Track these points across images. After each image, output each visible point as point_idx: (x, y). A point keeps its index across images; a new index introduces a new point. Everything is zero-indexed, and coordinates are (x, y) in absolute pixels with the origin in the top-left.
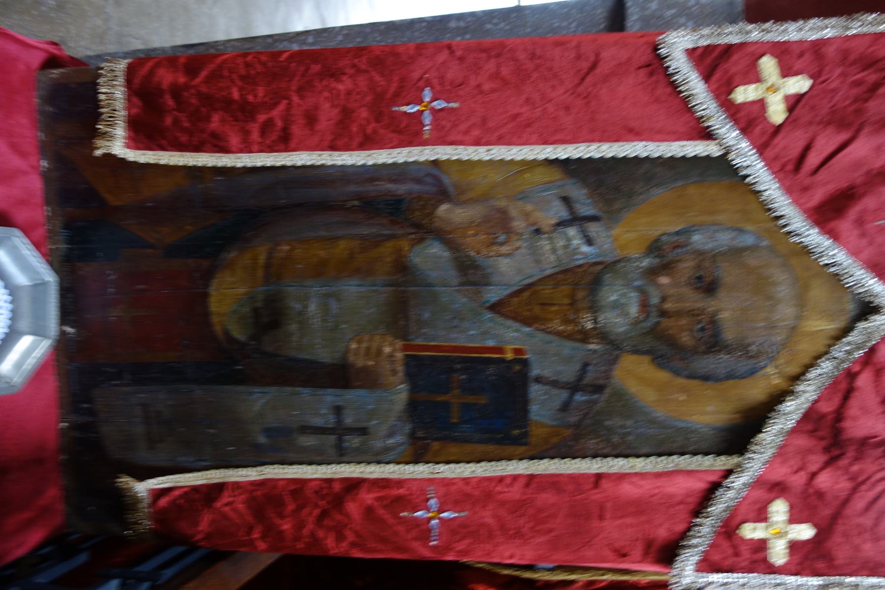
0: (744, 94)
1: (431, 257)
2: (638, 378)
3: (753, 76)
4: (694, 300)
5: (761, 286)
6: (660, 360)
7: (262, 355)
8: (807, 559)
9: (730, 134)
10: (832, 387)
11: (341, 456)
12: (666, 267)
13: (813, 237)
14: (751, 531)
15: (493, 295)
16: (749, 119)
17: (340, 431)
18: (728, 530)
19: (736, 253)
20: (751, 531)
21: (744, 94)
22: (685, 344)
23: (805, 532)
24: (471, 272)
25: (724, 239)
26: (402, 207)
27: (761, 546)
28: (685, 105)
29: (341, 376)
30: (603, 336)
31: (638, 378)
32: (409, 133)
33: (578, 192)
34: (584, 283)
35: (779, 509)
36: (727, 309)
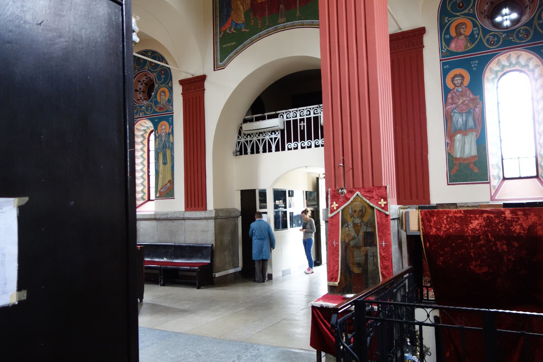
0: (335, 208)
1: (352, 243)
2: (366, 219)
3: (333, 208)
4: (357, 213)
5: (355, 206)
6: (363, 217)
7: (364, 266)
8: (385, 199)
9: (339, 210)
10: (366, 198)
11: (377, 256)
12: (353, 216)
13: (350, 201)
14: (383, 206)
15: (356, 236)
16: (338, 208)
17: (373, 256)
18: (383, 208)
19: (352, 208)
20: (383, 206)
21: (335, 208)
22: (362, 213)
23: (382, 200)
24: (354, 238)
25: (350, 210)
26: (346, 247)
27: (385, 204)
28: (336, 214)
29: (366, 255)
30: (361, 223)
31: (366, 219)
32: (337, 245)
33: (345, 226)
34: (355, 225)
35: (379, 203)
36: (358, 209)
